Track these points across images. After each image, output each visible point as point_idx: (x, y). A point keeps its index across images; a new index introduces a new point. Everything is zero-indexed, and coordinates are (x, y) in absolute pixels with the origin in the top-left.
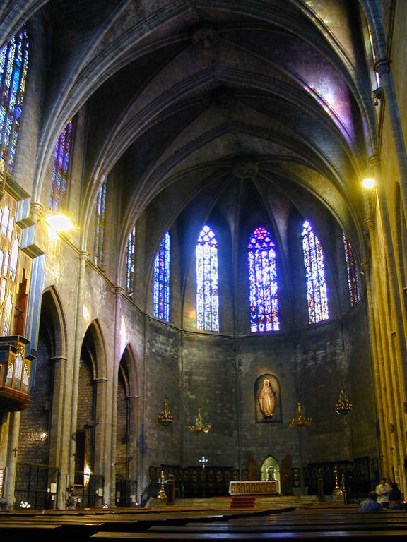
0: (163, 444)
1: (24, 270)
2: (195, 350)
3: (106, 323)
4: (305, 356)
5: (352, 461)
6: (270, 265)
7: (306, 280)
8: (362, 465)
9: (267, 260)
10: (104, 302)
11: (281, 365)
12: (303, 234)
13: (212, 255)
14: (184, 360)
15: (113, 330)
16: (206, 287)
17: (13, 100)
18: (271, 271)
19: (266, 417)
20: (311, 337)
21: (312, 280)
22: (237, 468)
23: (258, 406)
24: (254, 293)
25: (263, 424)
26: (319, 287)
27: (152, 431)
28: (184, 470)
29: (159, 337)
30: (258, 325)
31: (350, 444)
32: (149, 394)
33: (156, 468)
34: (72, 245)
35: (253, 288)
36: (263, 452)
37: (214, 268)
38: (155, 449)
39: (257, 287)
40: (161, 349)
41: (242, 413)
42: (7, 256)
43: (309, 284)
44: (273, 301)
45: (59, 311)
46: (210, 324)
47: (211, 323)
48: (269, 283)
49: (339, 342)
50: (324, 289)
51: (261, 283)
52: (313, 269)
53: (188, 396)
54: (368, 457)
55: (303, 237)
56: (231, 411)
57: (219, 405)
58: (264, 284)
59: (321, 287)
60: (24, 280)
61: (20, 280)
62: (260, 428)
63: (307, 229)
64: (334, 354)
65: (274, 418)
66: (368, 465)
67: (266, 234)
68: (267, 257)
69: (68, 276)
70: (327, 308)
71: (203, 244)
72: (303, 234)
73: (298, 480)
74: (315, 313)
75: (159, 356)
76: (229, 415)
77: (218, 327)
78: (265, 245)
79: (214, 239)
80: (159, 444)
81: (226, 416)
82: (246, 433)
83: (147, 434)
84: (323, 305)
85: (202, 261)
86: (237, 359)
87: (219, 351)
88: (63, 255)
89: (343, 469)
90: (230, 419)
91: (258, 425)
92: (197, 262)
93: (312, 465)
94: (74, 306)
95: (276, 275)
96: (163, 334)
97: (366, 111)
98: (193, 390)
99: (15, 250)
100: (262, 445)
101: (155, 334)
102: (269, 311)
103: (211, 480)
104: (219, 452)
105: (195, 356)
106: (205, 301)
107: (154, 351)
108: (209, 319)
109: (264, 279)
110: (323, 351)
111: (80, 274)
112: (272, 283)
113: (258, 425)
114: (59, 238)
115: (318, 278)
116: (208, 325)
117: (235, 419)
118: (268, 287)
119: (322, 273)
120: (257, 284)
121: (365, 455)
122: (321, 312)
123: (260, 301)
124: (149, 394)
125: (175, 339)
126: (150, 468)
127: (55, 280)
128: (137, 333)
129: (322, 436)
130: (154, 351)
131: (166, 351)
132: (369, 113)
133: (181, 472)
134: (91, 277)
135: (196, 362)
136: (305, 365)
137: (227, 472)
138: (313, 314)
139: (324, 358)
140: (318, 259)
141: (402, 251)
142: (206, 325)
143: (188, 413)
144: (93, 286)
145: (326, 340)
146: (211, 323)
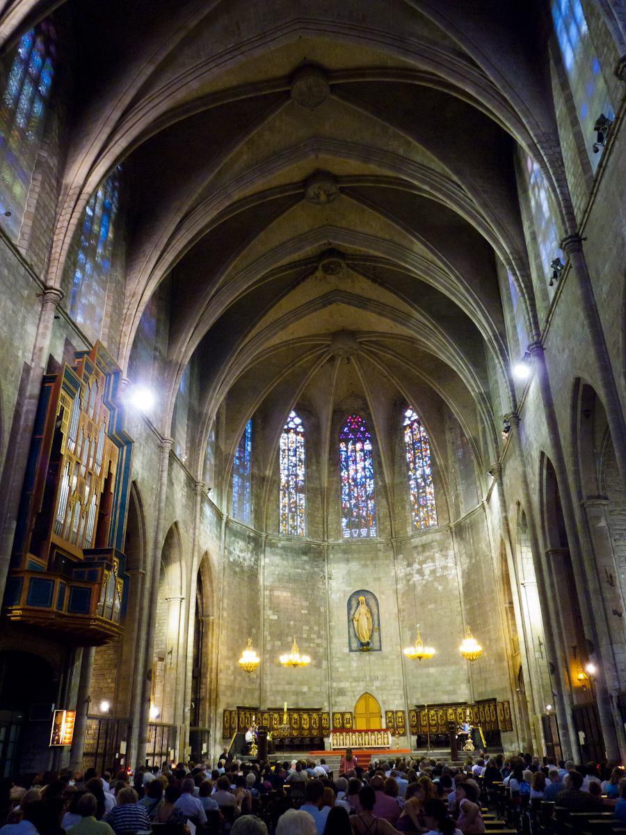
0: (239, 678)
1: (110, 462)
2: (277, 560)
3: (186, 527)
4: (409, 569)
5: (473, 702)
6: (365, 460)
7: (409, 478)
8: (487, 708)
9: (362, 454)
10: (184, 501)
11: (379, 579)
12: (405, 424)
13: (298, 445)
14: (266, 571)
15: (192, 535)
16: (291, 483)
17: (100, 250)
18: (367, 466)
19: (362, 644)
20: (416, 547)
21: (416, 479)
22: (326, 710)
23: (352, 630)
24: (347, 492)
25: (358, 653)
26: (424, 487)
27: (227, 662)
28: (263, 713)
29: (238, 543)
30: (351, 530)
31: (469, 681)
32: (225, 614)
33: (231, 712)
34: (154, 431)
35: (345, 485)
36: (359, 689)
37: (300, 460)
38: (231, 686)
39: (350, 485)
40: (239, 557)
41: (331, 637)
42: (93, 445)
43: (412, 482)
44: (369, 502)
45: (139, 512)
46: (294, 528)
47: (296, 526)
48: (364, 480)
49: (451, 553)
50: (430, 490)
51: (354, 480)
52: (417, 465)
53: (269, 616)
54: (495, 700)
55: (405, 428)
56: (320, 637)
57: (306, 628)
58: (358, 480)
59: (427, 487)
60: (110, 474)
61: (105, 476)
62: (355, 658)
63: (409, 418)
64: (445, 568)
65: (371, 645)
66: (496, 710)
67: (362, 422)
68: (362, 450)
69: (150, 468)
70: (434, 512)
71: (288, 431)
72: (405, 424)
73: (404, 727)
74: (420, 518)
75: (238, 566)
76: (318, 641)
77: (304, 531)
78: (359, 435)
79: (300, 427)
80: (235, 679)
81: (314, 643)
82: (338, 665)
83: (221, 666)
84: (429, 508)
85: (286, 451)
86: (326, 571)
87: (305, 561)
88: (146, 443)
89: (460, 714)
90: (318, 645)
91: (353, 654)
92: (281, 453)
93: (421, 707)
94: (155, 506)
95: (372, 471)
96: (244, 540)
97: (524, 291)
98: (275, 608)
99: (102, 438)
100: (357, 680)
101: (233, 538)
102: (364, 514)
103: (295, 726)
104: (305, 689)
105: (278, 565)
106: (290, 499)
107: (231, 560)
108: (294, 521)
109: (359, 476)
110: (432, 564)
111: (162, 466)
112: (368, 480)
113: (351, 653)
114: (143, 422)
115: (423, 476)
116: (293, 528)
117: (325, 646)
118: (363, 485)
119: (428, 471)
120: (350, 481)
121: (491, 697)
122: (428, 516)
123: (353, 502)
124: (225, 614)
125: (255, 546)
126: (225, 711)
127: (138, 474)
128: (215, 538)
129: (432, 670)
130: (231, 560)
131: (244, 559)
132: (528, 293)
133: (259, 715)
134: (172, 469)
135: (279, 574)
136: (409, 581)
137: (315, 716)
138: (417, 518)
139: (433, 572)
140: (424, 453)
141: (577, 456)
142: (290, 529)
143: (269, 638)
144: (174, 481)
145: (435, 550)
146: (296, 526)
